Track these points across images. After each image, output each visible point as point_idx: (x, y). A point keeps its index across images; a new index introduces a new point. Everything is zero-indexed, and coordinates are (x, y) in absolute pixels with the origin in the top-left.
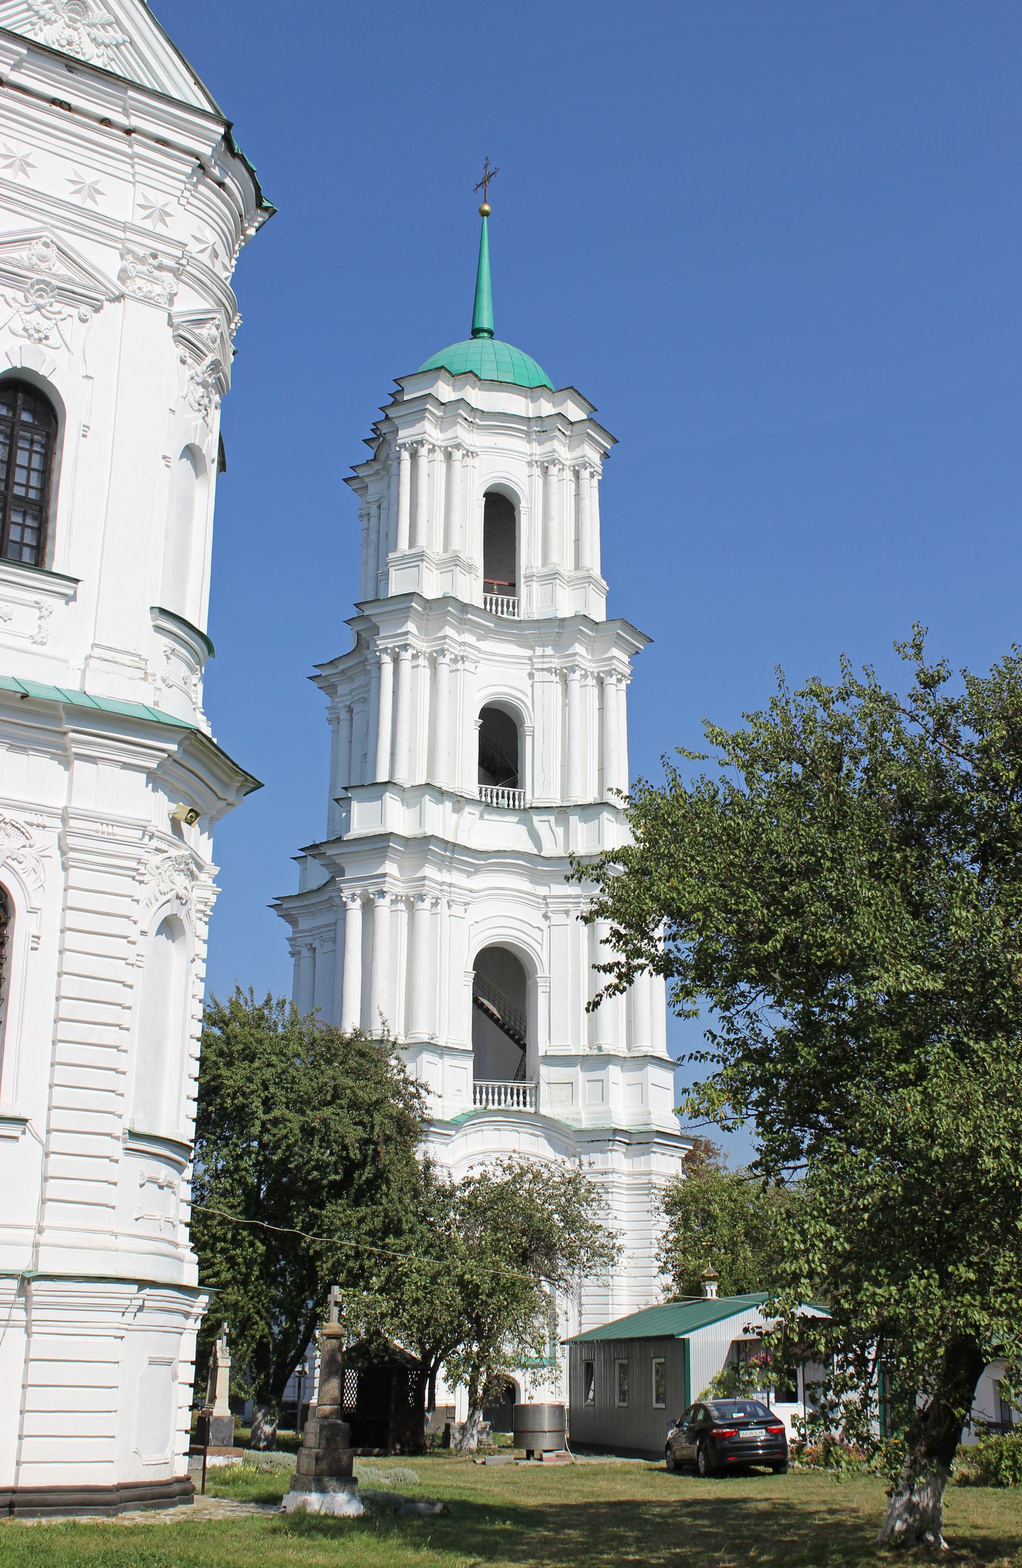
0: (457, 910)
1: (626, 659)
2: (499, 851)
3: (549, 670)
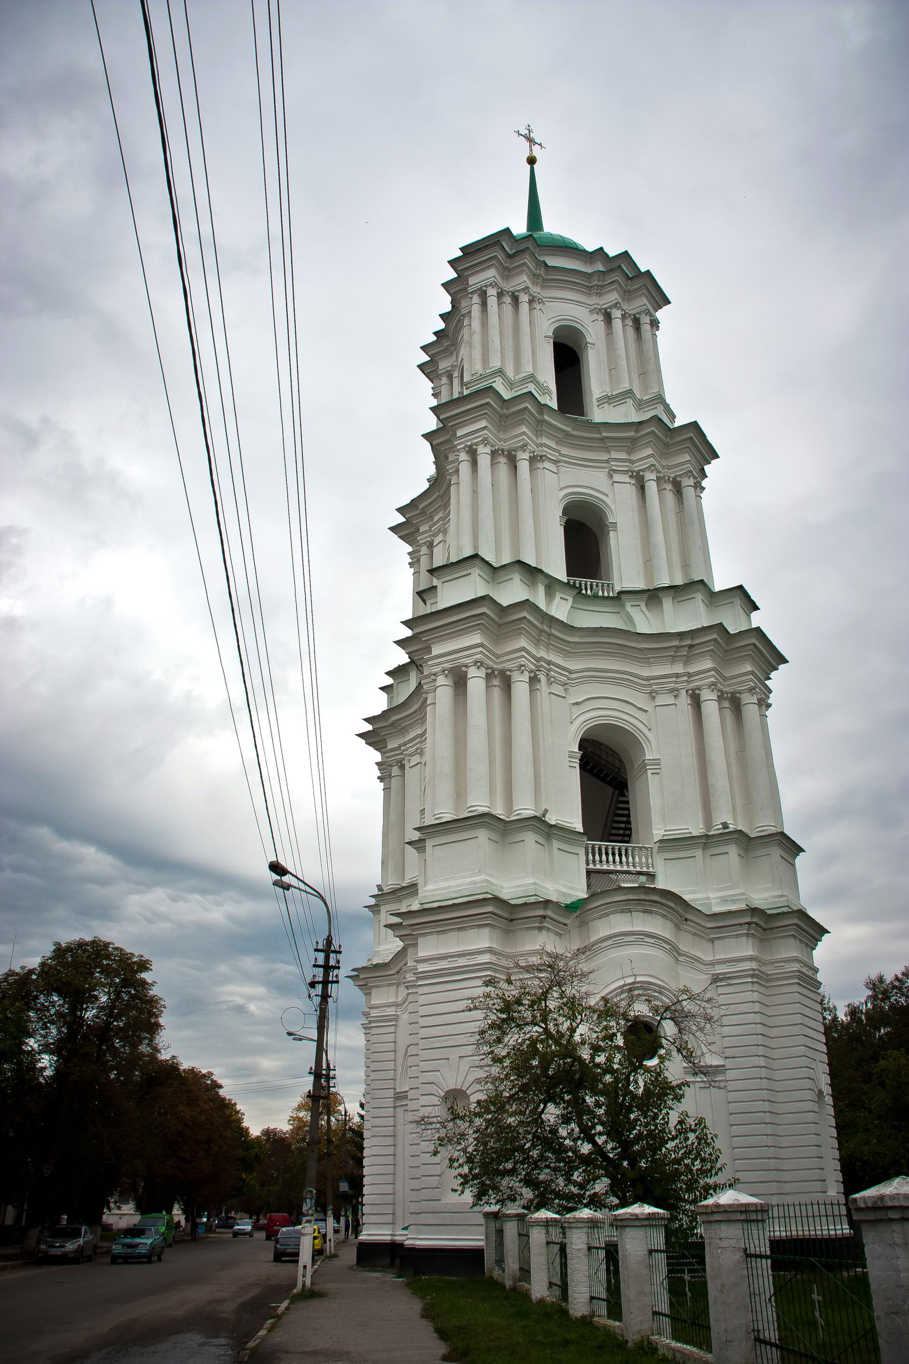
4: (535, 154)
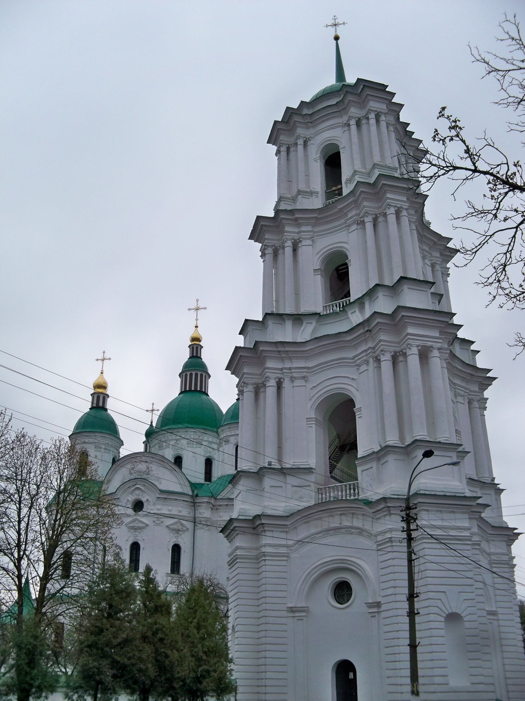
0: (297, 383)
4: (339, 34)
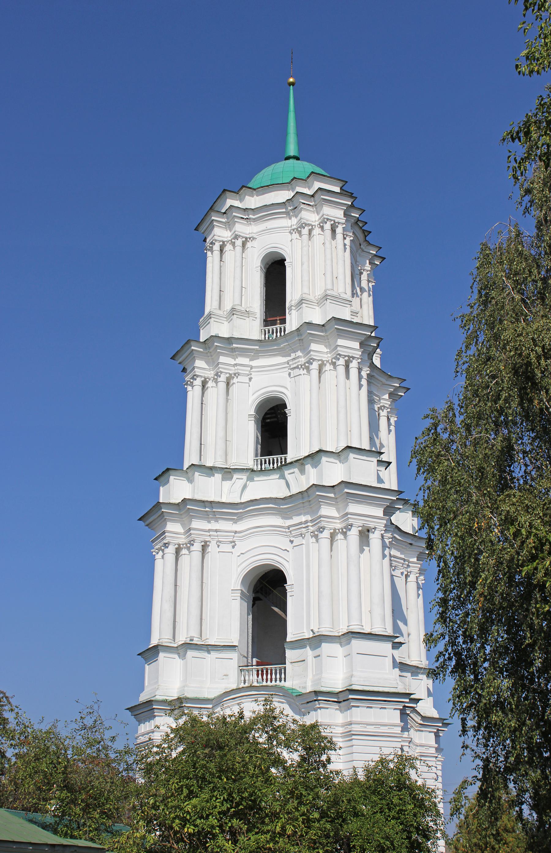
1: (356, 345)
2: (252, 501)
3: (297, 367)
